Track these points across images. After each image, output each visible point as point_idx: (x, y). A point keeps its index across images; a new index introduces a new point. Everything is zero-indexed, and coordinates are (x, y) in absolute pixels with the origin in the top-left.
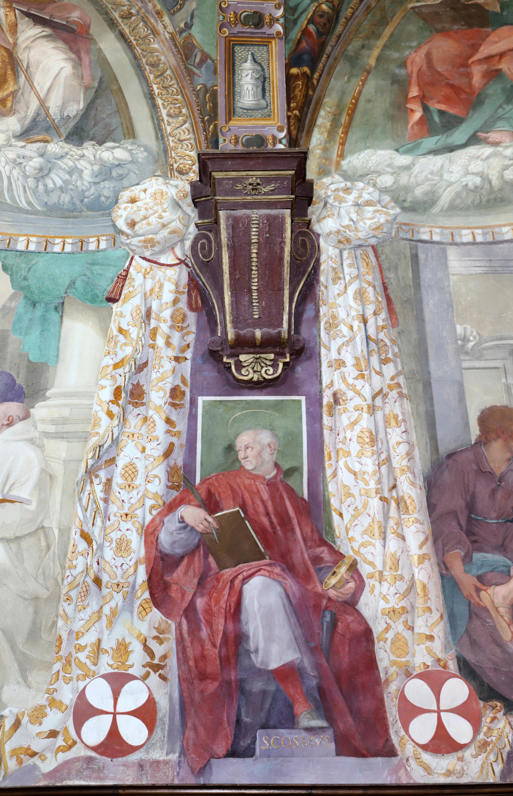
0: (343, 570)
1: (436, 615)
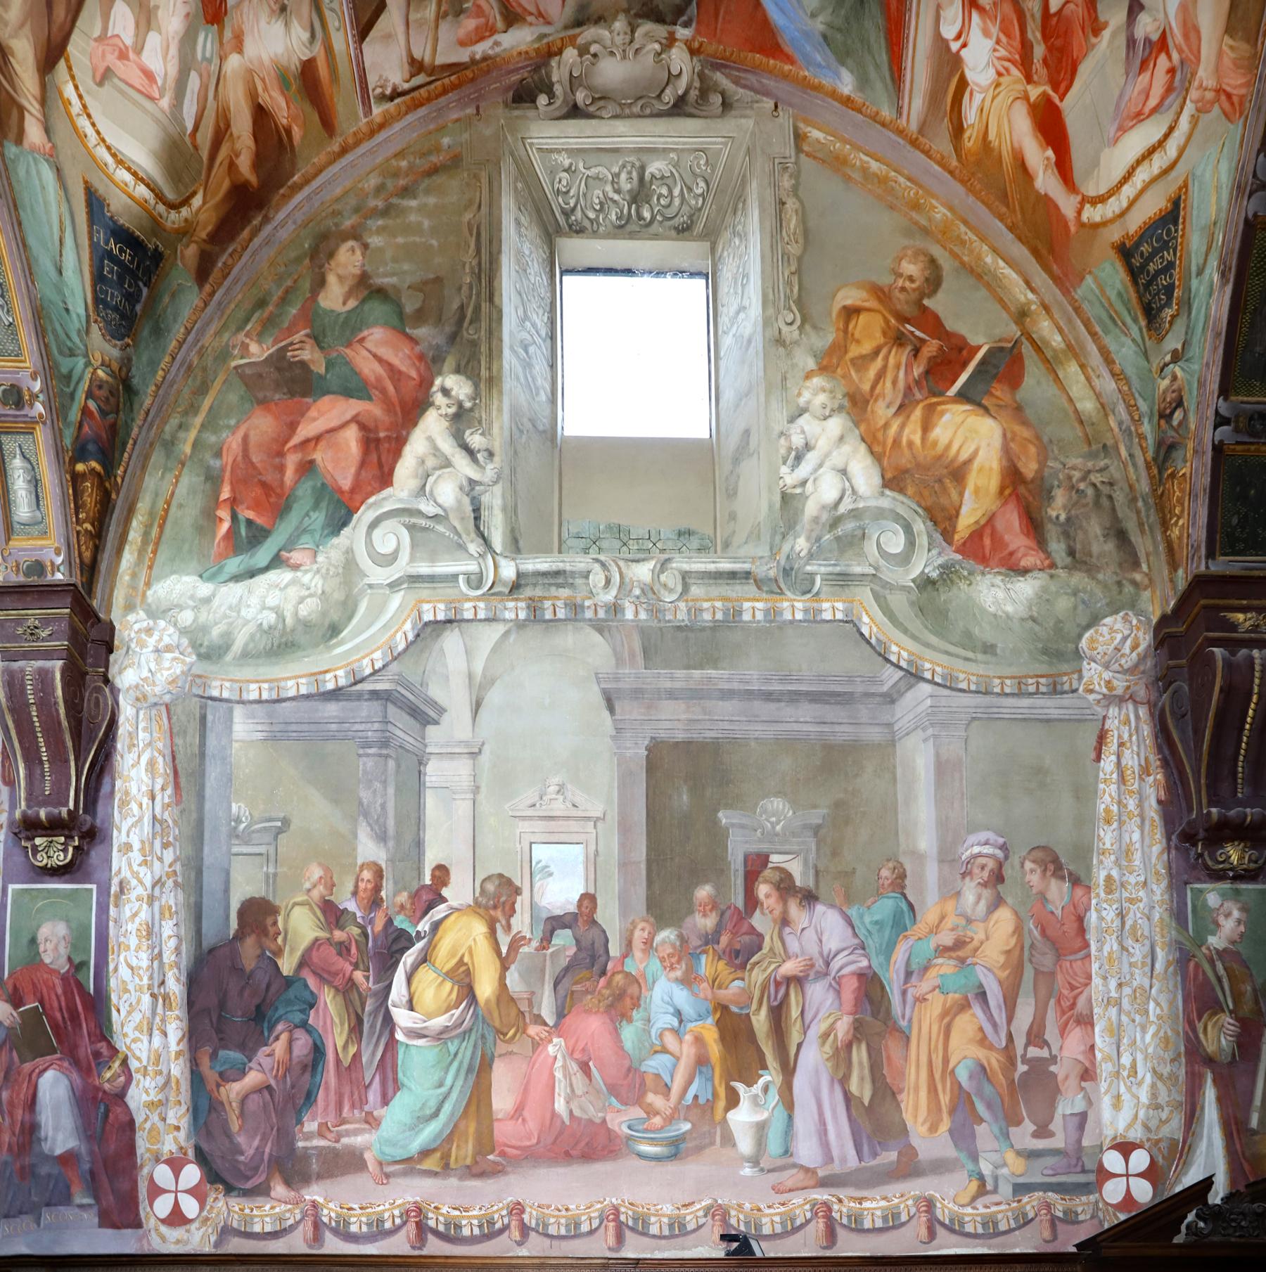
0: (116, 1064)
1: (184, 1108)
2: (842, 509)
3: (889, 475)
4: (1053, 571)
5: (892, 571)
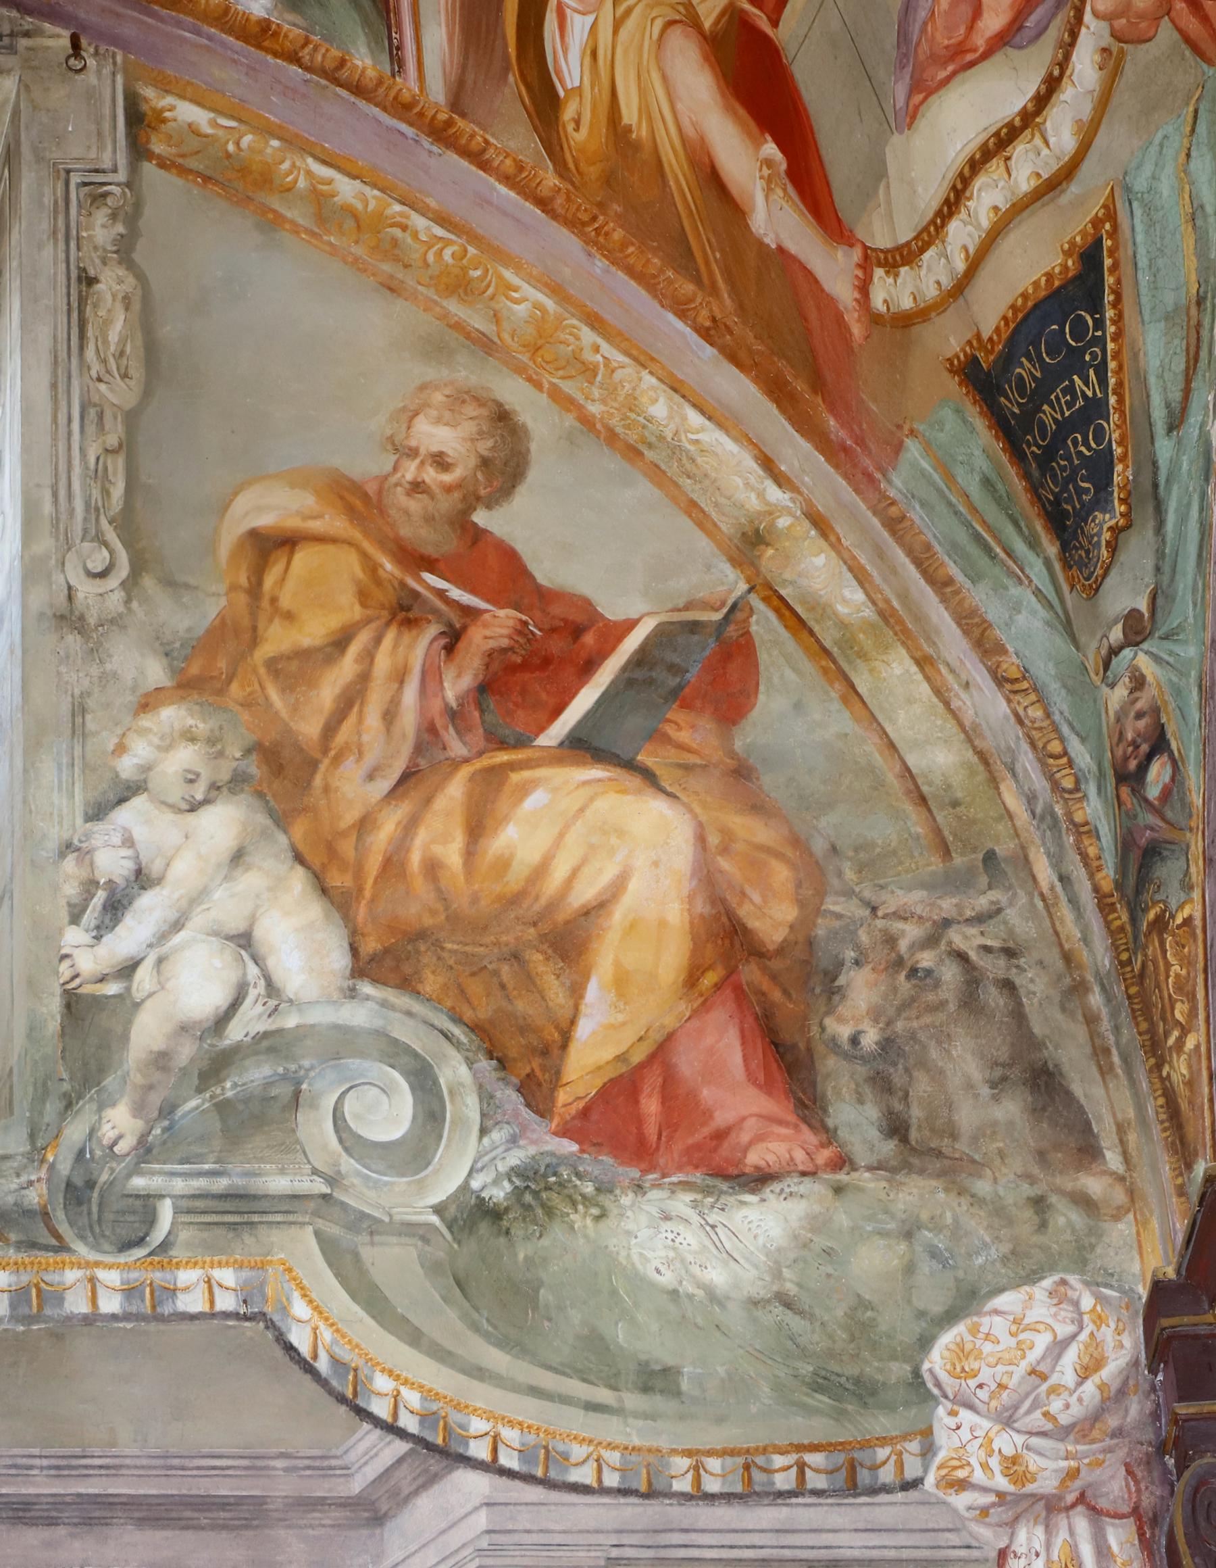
2: (236, 1032)
3: (370, 946)
4: (842, 1177)
5: (376, 1185)
